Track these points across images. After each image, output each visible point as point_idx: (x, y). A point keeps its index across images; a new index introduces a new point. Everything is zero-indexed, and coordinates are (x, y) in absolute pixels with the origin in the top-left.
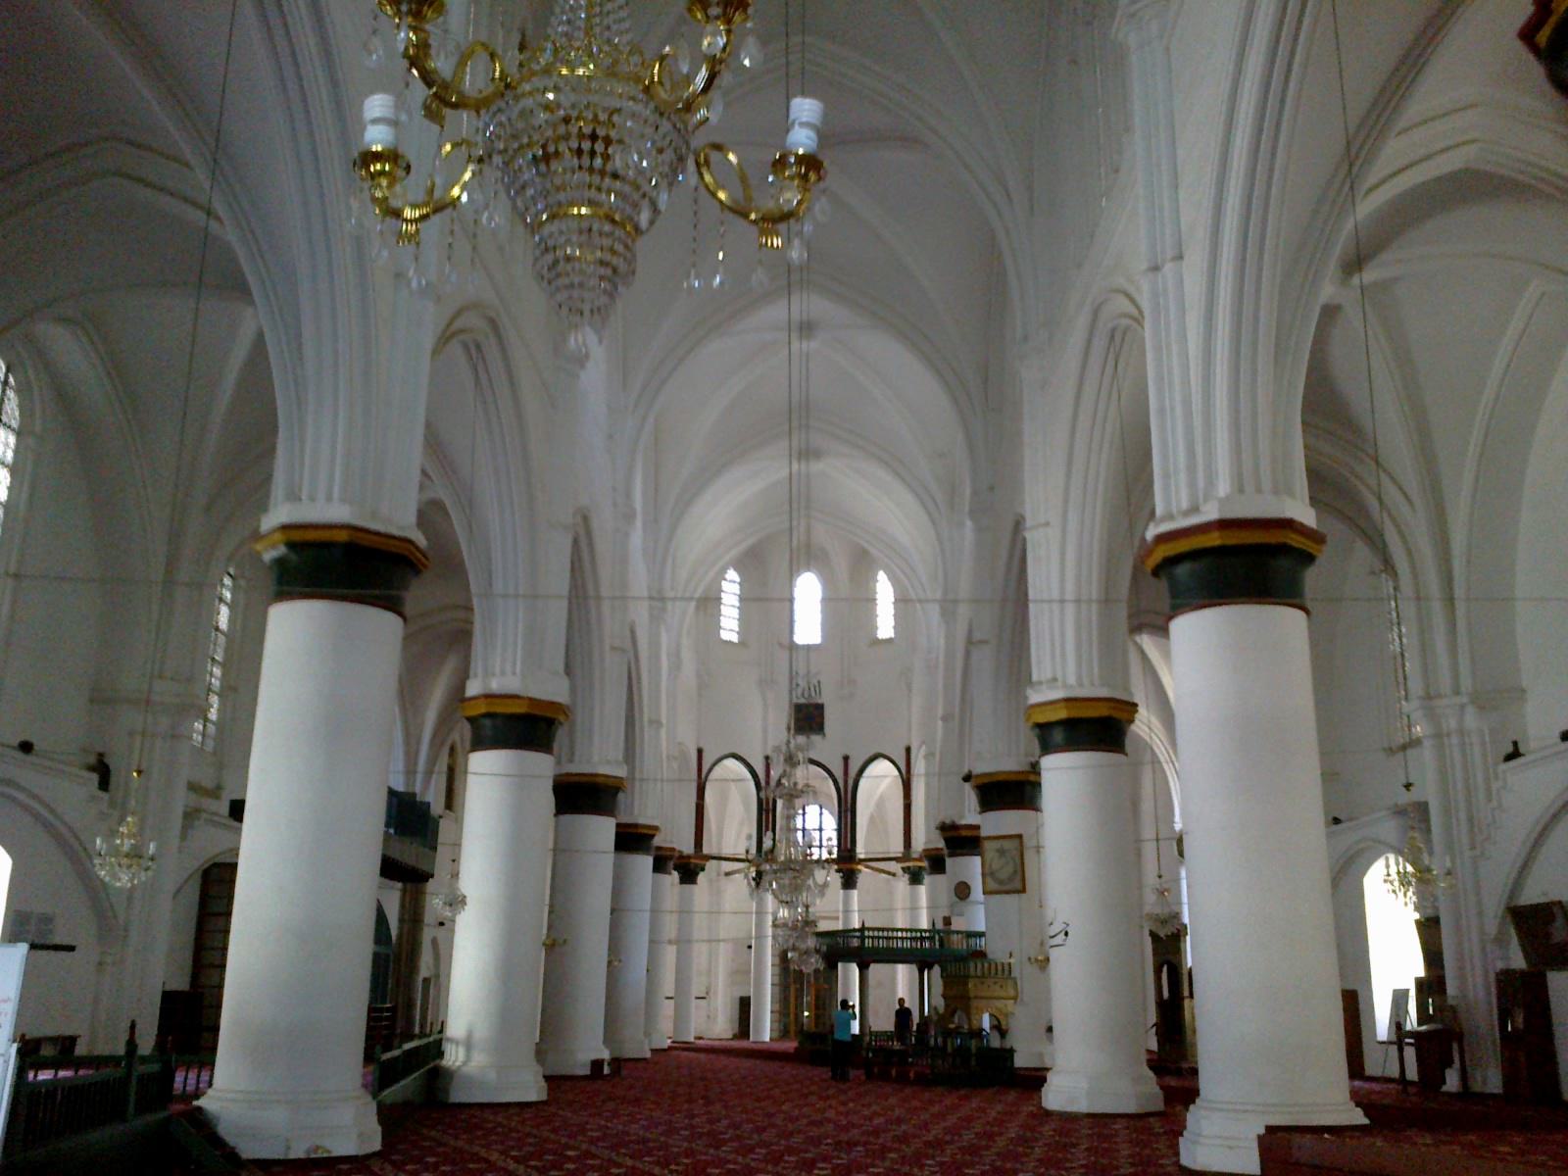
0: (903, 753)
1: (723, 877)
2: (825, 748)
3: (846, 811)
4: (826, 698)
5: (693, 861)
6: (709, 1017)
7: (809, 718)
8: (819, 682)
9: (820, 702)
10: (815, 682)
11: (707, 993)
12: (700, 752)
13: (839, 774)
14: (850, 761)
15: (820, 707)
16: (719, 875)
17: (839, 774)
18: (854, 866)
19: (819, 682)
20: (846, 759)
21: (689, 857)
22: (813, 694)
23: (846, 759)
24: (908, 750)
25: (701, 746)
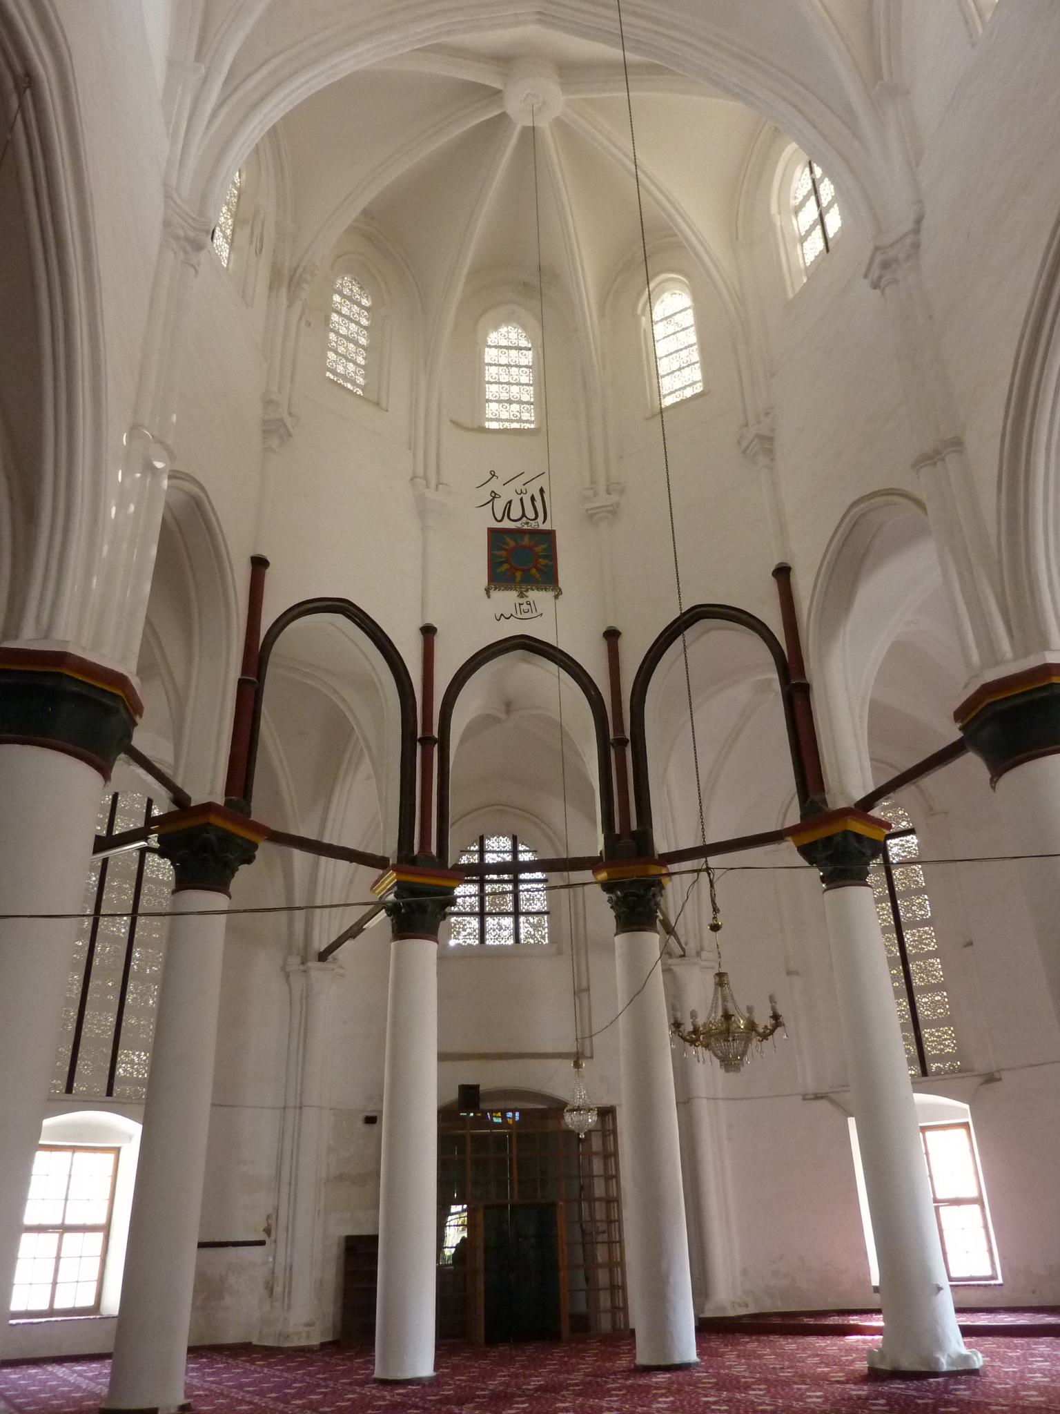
0: (771, 587)
1: (314, 965)
2: (564, 618)
3: (621, 742)
4: (560, 521)
5: (215, 820)
6: (270, 1290)
7: (522, 557)
8: (542, 491)
9: (542, 527)
10: (534, 489)
11: (268, 1231)
12: (259, 564)
13: (594, 663)
14: (624, 644)
15: (550, 535)
16: (304, 962)
17: (594, 663)
18: (654, 870)
19: (542, 491)
20: (612, 636)
21: (208, 807)
22: (530, 513)
23: (612, 636)
24: (783, 573)
25: (263, 552)
